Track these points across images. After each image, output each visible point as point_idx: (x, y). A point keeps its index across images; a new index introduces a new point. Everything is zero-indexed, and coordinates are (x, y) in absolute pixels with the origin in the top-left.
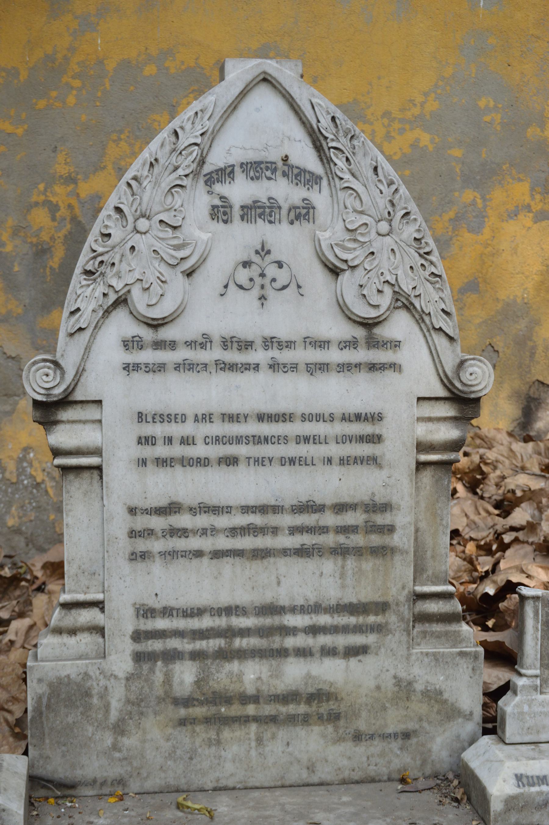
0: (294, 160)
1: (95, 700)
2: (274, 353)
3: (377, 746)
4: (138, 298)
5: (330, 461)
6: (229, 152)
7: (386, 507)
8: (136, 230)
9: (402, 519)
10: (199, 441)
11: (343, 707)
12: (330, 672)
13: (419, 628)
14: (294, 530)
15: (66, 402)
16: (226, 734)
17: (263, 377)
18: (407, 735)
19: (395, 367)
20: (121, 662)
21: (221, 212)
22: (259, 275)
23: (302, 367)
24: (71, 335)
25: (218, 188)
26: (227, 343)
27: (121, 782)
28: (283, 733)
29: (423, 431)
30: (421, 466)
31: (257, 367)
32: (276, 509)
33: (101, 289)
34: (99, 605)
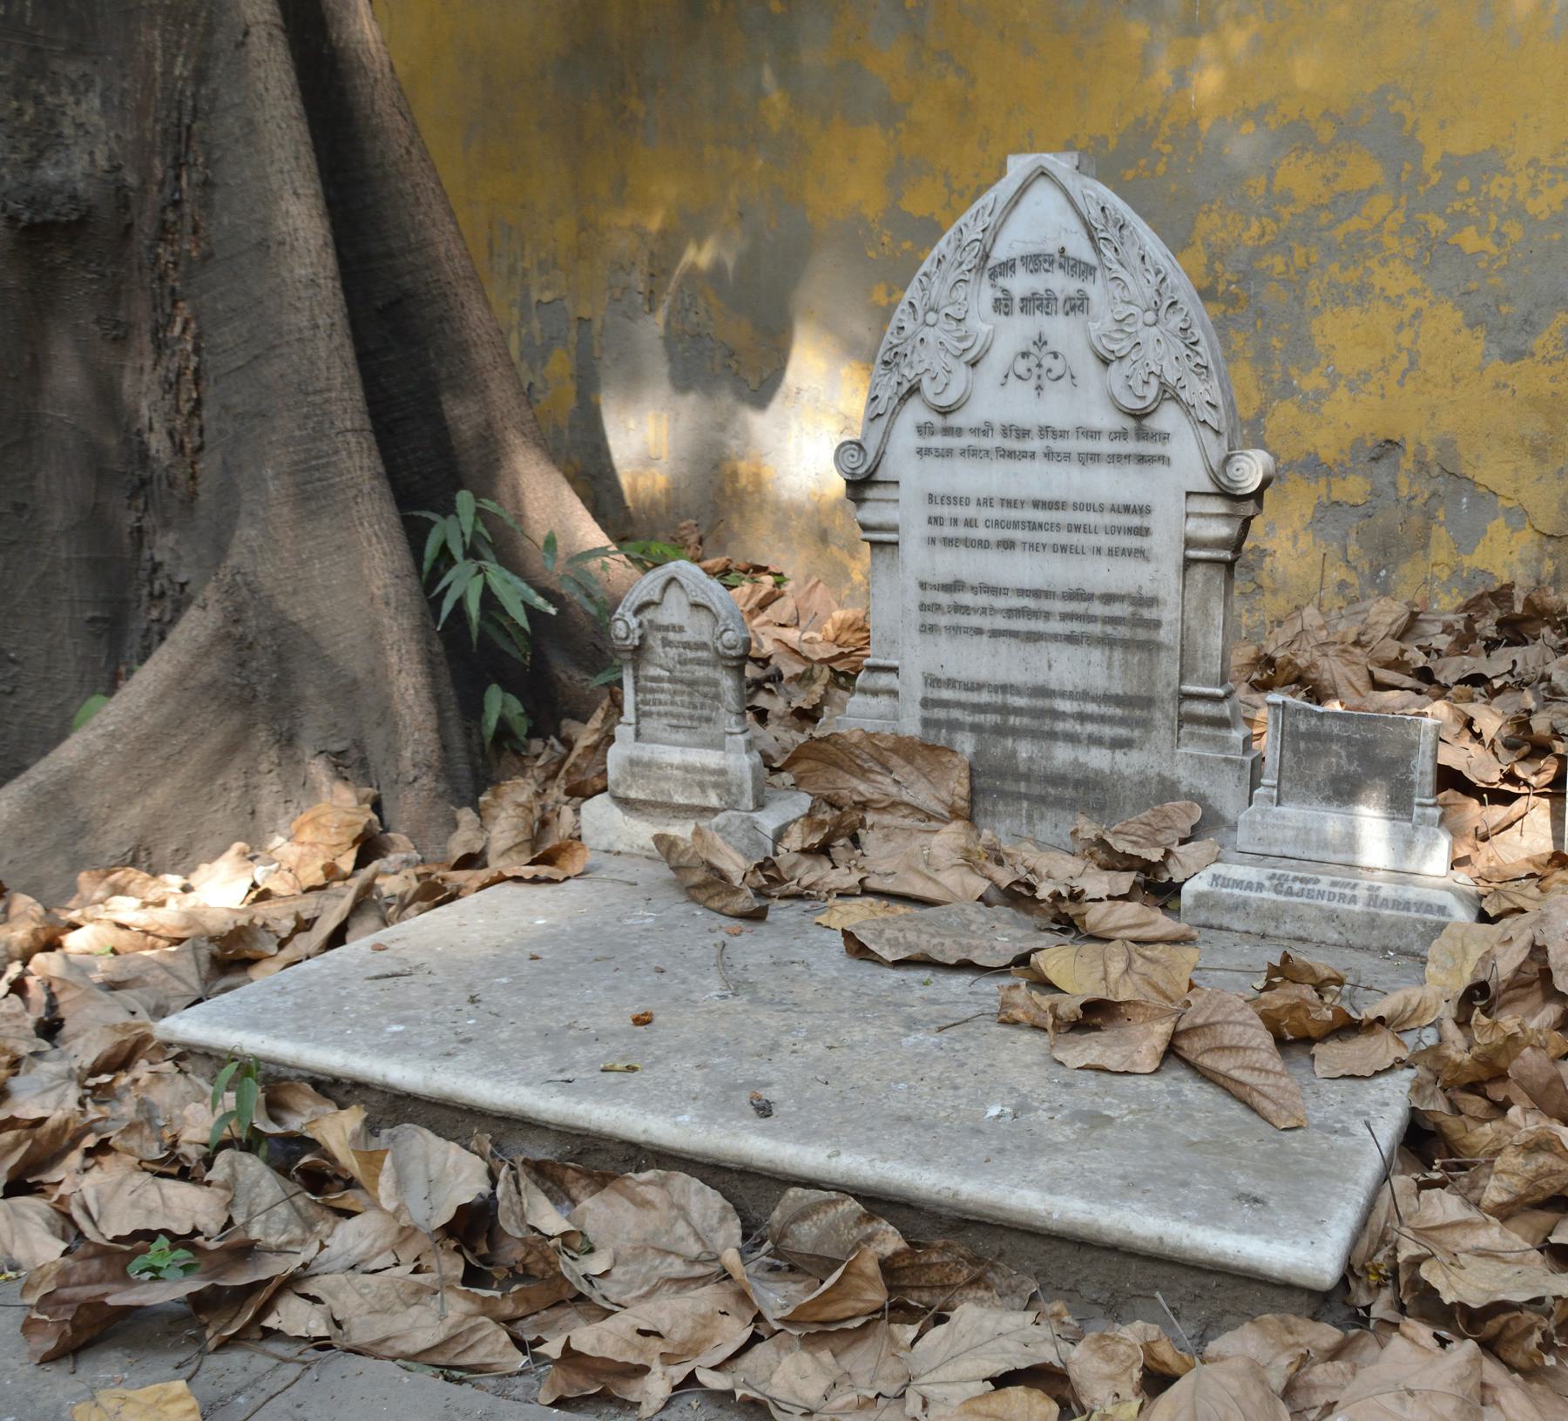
0: (1070, 252)
2: (1049, 442)
4: (927, 387)
5: (1099, 550)
6: (1010, 246)
7: (1152, 602)
8: (925, 323)
9: (1169, 614)
10: (981, 523)
13: (1187, 728)
14: (1065, 617)
17: (1039, 465)
19: (1164, 459)
21: (1003, 305)
22: (1038, 367)
23: (1075, 457)
24: (872, 420)
25: (1001, 281)
26: (1007, 431)
30: (1189, 563)
31: (1033, 455)
32: (1048, 595)
33: (896, 378)
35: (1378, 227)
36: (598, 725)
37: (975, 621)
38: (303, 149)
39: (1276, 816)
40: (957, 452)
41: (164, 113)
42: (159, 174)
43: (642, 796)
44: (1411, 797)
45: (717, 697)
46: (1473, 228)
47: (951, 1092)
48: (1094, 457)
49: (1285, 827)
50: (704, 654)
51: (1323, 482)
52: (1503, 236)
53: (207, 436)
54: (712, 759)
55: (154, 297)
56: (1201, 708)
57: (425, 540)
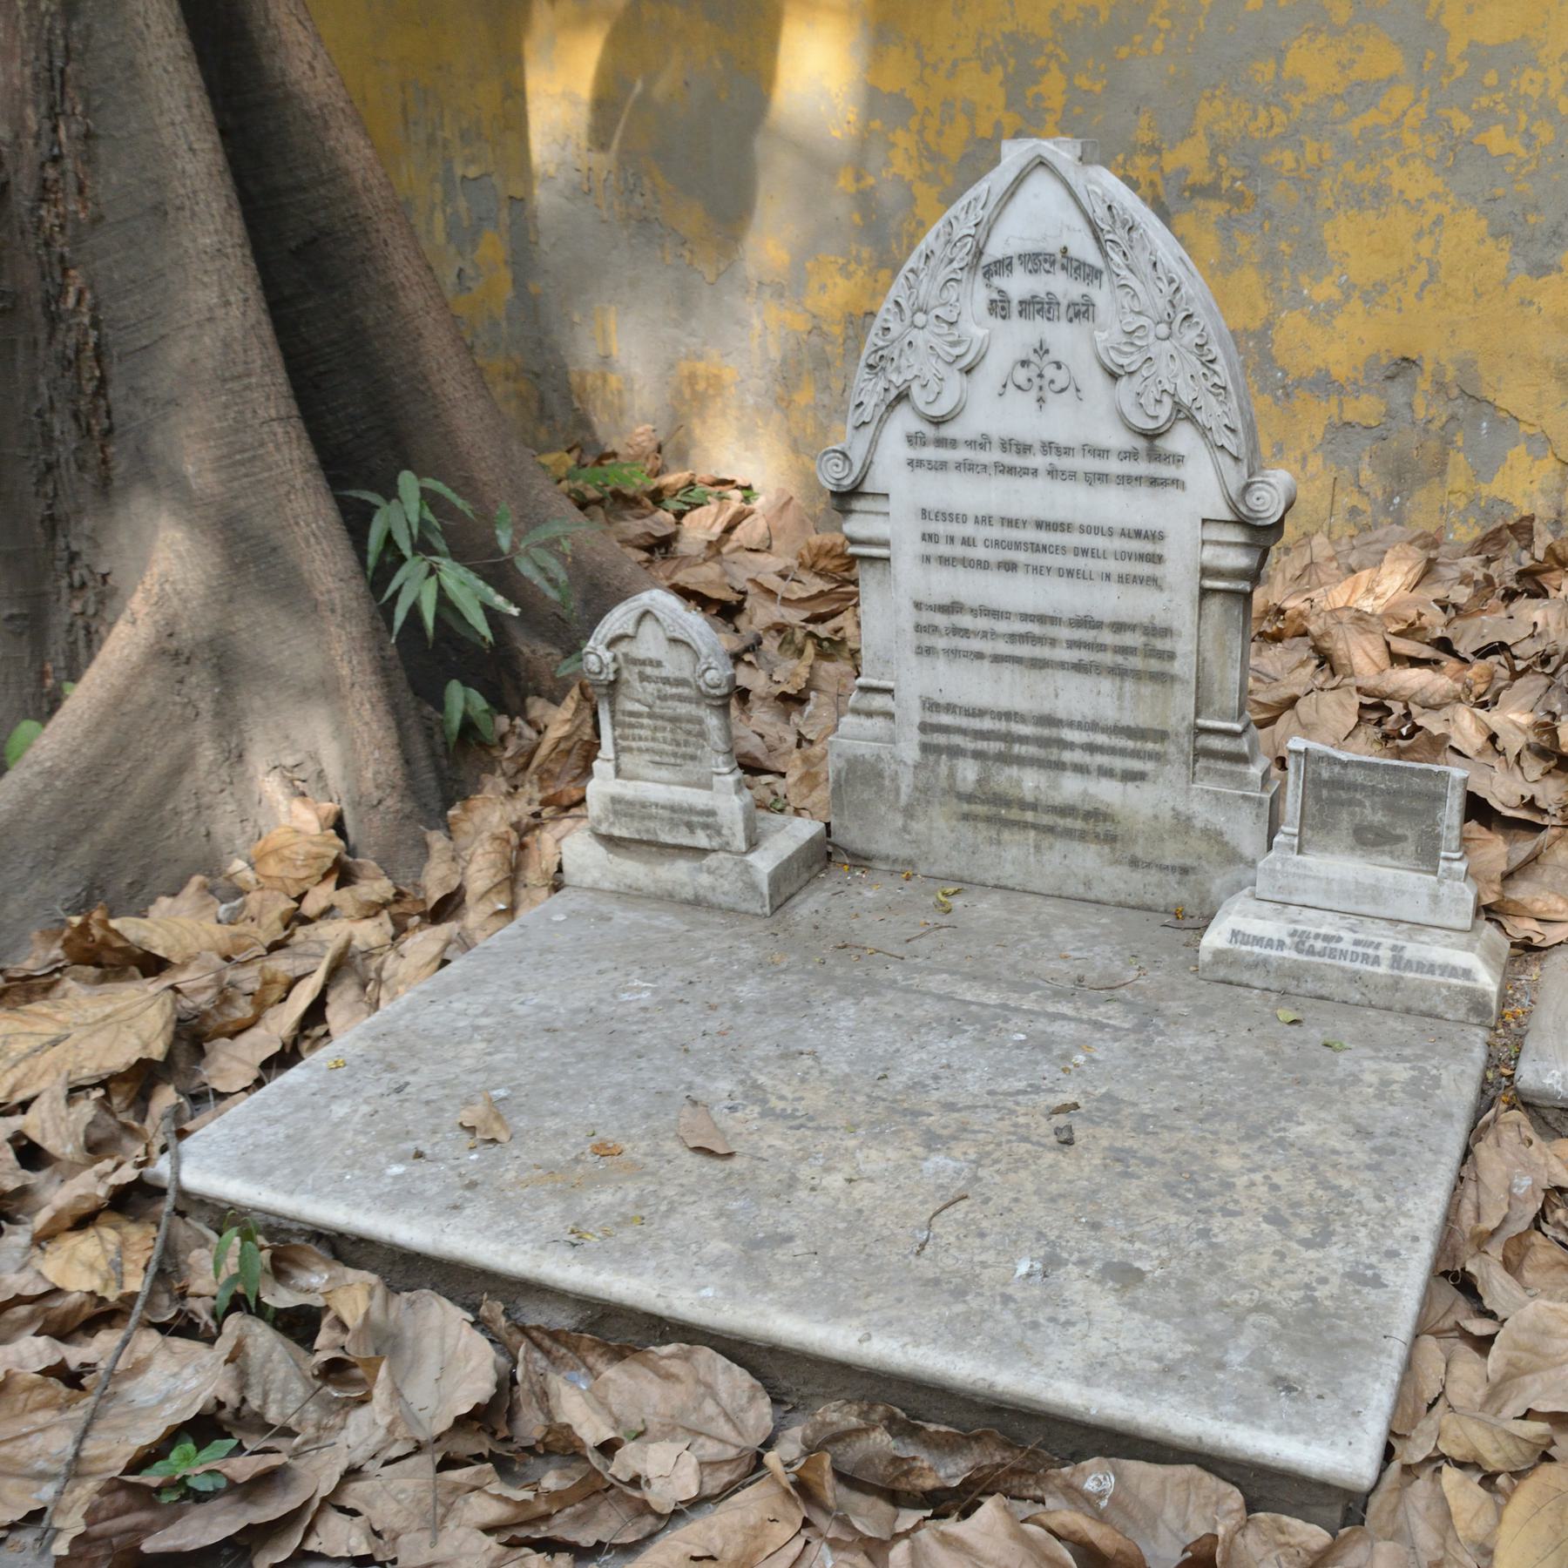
0: (1072, 253)
1: (887, 782)
2: (1052, 459)
3: (1154, 876)
5: (1108, 577)
7: (1166, 632)
9: (1184, 646)
10: (980, 543)
11: (1119, 831)
12: (1108, 792)
13: (1202, 762)
14: (1072, 644)
15: (855, 492)
16: (1006, 835)
17: (1042, 482)
18: (1185, 871)
19: (1177, 483)
20: (909, 750)
21: (999, 307)
22: (1038, 375)
23: (1080, 476)
25: (997, 281)
26: (1006, 445)
27: (910, 862)
28: (1060, 845)
29: (1210, 555)
30: (1205, 593)
32: (1054, 620)
33: (882, 384)
34: (889, 691)
35: (1397, 123)
36: (568, 715)
37: (976, 644)
38: (195, 95)
39: (1297, 865)
40: (952, 466)
41: (32, 55)
42: (32, 123)
43: (625, 833)
44: (1437, 849)
45: (702, 735)
46: (1500, 127)
47: (978, 1242)
48: (1102, 478)
49: (1306, 876)
50: (685, 691)
51: (1334, 401)
52: (1532, 137)
53: (116, 418)
54: (698, 798)
55: (40, 263)
56: (1216, 743)
57: (365, 537)
